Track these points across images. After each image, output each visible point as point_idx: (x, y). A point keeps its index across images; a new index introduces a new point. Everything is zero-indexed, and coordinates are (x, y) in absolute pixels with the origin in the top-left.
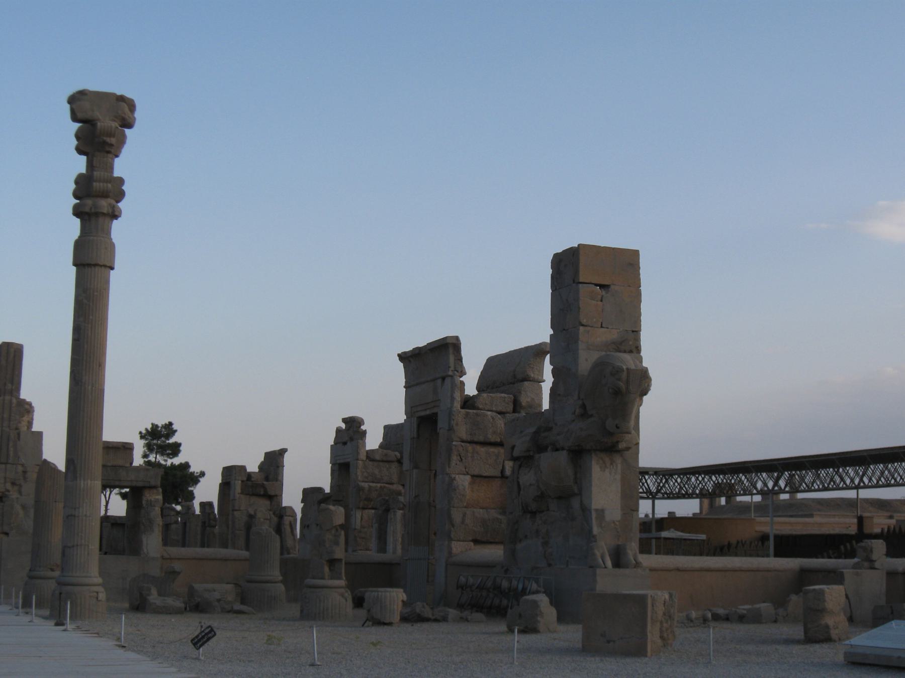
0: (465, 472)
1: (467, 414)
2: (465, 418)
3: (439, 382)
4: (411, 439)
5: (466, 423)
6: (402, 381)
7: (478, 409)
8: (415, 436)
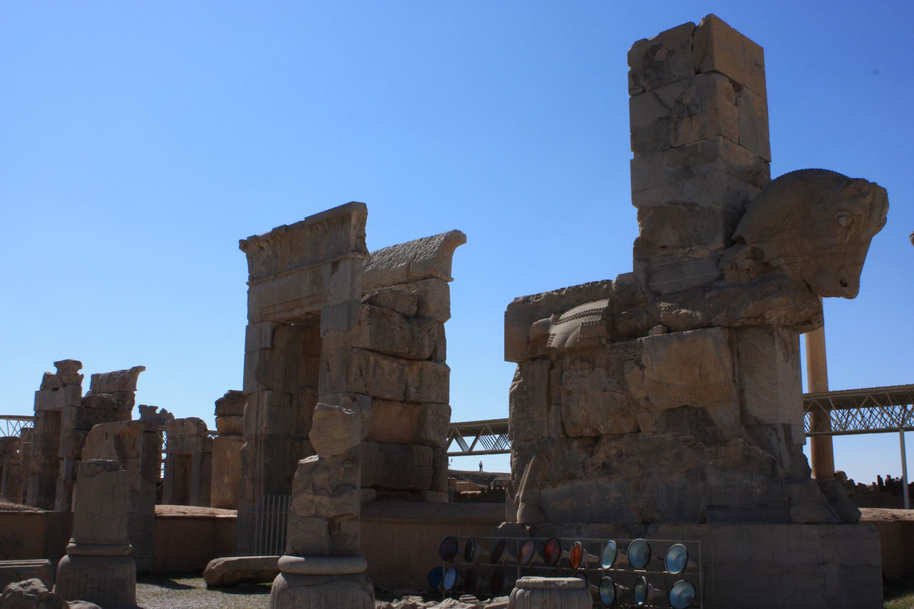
1: (371, 311)
2: (369, 317)
3: (326, 269)
5: (369, 324)
6: (245, 275)
7: (383, 307)
8: (268, 345)
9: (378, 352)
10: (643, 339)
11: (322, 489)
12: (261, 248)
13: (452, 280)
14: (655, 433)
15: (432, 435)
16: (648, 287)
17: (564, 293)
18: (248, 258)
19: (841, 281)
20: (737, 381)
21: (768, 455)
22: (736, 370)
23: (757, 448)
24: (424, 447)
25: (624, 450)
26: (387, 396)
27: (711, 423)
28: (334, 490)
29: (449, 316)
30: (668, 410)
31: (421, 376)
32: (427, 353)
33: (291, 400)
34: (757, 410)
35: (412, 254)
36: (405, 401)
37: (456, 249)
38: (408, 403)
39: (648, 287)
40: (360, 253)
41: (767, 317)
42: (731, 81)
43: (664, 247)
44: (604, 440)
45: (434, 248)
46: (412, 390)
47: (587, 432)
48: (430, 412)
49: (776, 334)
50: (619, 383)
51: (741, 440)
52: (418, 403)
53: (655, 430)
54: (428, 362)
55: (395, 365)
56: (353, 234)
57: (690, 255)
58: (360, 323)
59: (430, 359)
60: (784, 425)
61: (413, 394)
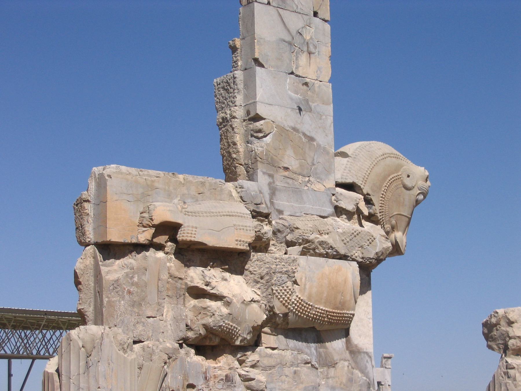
21: (365, 378)
39: (272, 203)
43: (286, 169)
51: (346, 363)
57: (309, 185)
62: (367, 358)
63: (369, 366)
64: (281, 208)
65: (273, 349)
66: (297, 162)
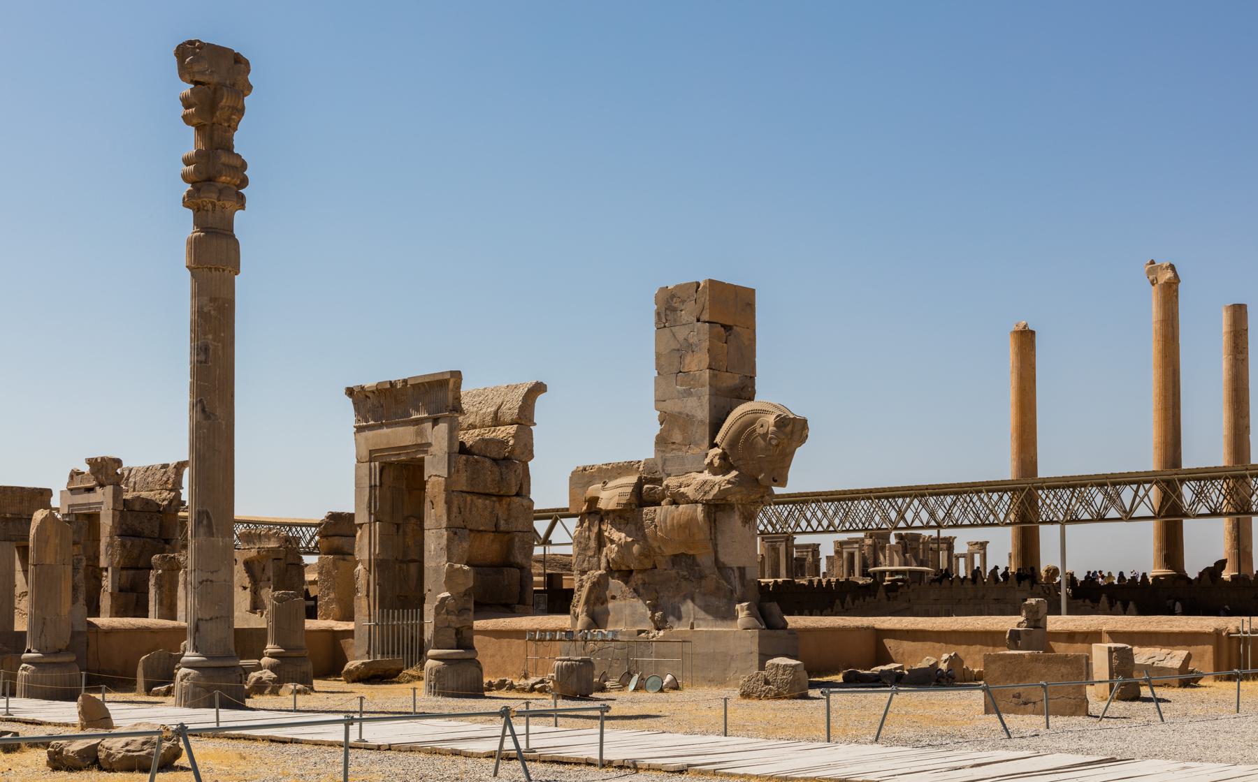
0: (463, 526)
1: (467, 461)
2: (465, 465)
4: (371, 487)
8: (378, 484)
9: (473, 493)
10: (657, 507)
11: (452, 611)
12: (367, 396)
13: (535, 424)
14: (666, 569)
15: (519, 558)
16: (664, 470)
17: (610, 467)
18: (355, 404)
19: (773, 478)
20: (713, 538)
22: (713, 532)
23: (723, 582)
24: (512, 569)
25: (646, 580)
26: (481, 529)
27: (698, 565)
28: (459, 612)
29: (532, 457)
30: (673, 555)
31: (509, 510)
32: (514, 491)
33: (398, 529)
34: (723, 558)
35: (499, 401)
36: (497, 531)
37: (538, 399)
38: (498, 532)
39: (664, 470)
40: (457, 412)
41: (729, 499)
42: (723, 326)
43: (674, 443)
44: (634, 574)
45: (519, 397)
46: (502, 522)
47: (624, 568)
48: (517, 539)
49: (736, 509)
50: (642, 536)
51: (715, 576)
52: (508, 533)
53: (666, 567)
54: (515, 497)
55: (487, 502)
56: (450, 395)
58: (458, 471)
59: (518, 495)
60: (739, 568)
61: (503, 526)
62: (731, 571)
63: (732, 577)
64: (669, 472)
65: (666, 569)
66: (681, 436)
